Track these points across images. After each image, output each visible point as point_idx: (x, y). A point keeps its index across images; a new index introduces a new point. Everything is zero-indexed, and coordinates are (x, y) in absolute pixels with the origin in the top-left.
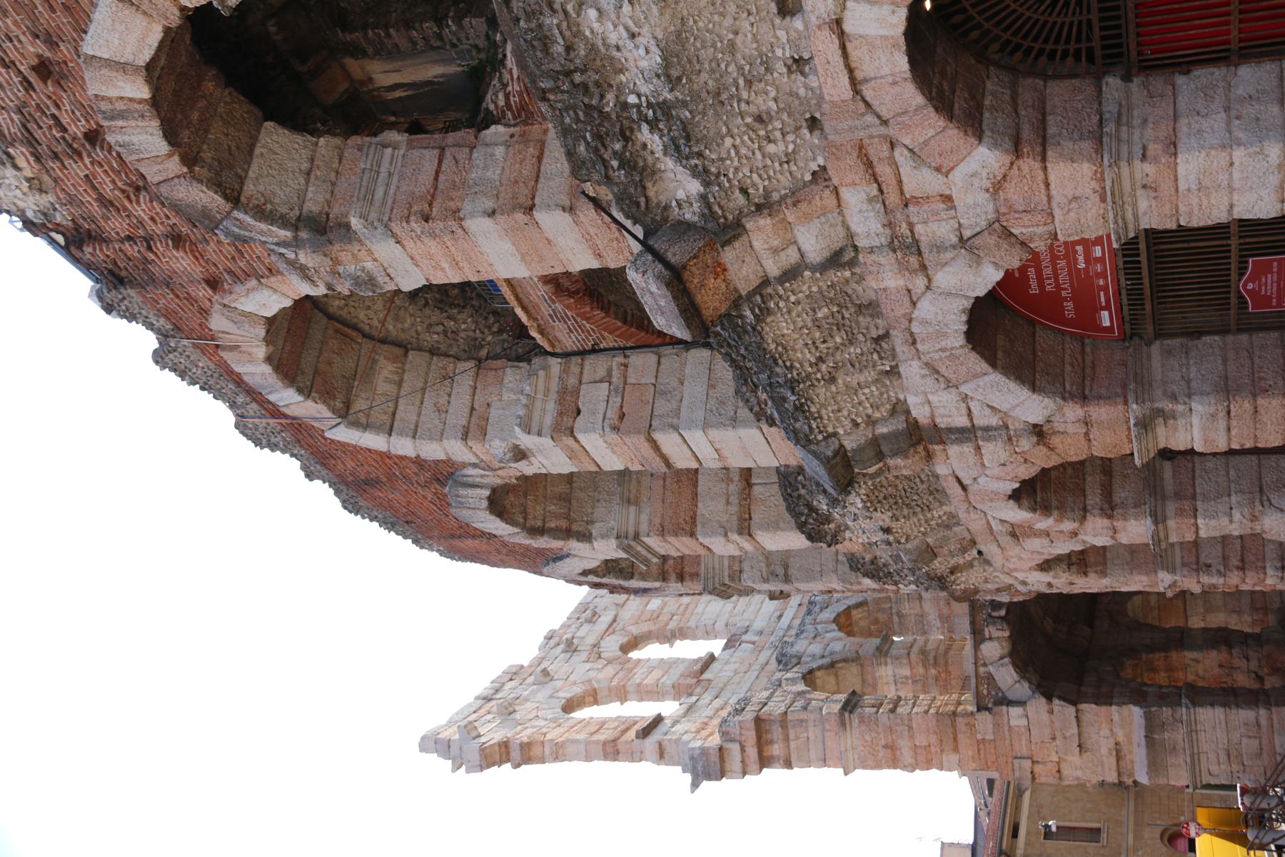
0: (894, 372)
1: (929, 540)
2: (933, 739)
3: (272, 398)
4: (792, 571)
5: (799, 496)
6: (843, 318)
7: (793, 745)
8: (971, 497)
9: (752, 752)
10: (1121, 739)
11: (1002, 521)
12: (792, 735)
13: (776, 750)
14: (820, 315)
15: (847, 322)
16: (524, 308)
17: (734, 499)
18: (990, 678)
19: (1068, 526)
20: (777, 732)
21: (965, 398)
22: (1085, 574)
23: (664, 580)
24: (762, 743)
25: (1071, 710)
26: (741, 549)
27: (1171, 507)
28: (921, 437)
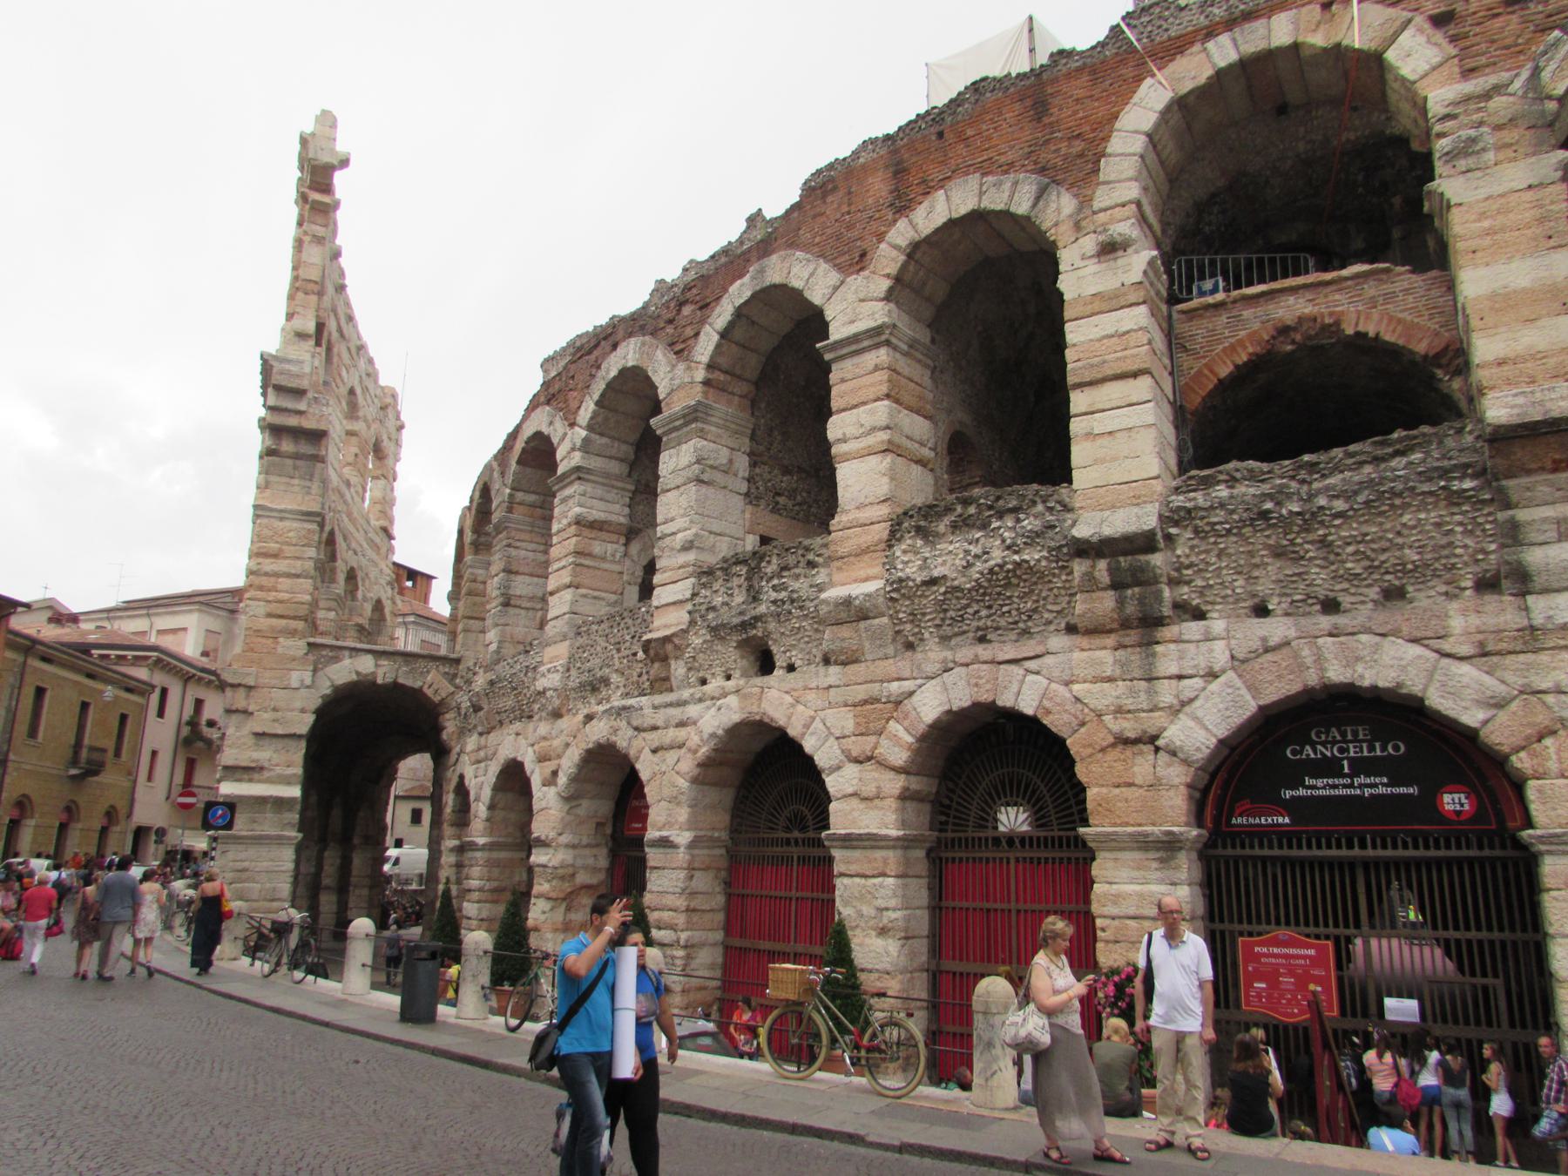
0: (1261, 611)
1: (885, 620)
2: (286, 596)
3: (1224, 39)
4: (704, 489)
5: (1034, 503)
6: (1387, 573)
7: (289, 462)
8: (985, 667)
9: (293, 421)
10: (266, 774)
11: (911, 694)
12: (299, 463)
13: (287, 446)
14: (1407, 551)
15: (1376, 576)
16: (1263, 294)
17: (909, 444)
18: (337, 659)
19: (900, 757)
20: (306, 448)
21: (1212, 675)
22: (699, 765)
23: (711, 366)
24: (297, 433)
25: (304, 729)
26: (844, 440)
27: (899, 852)
28: (1144, 626)
